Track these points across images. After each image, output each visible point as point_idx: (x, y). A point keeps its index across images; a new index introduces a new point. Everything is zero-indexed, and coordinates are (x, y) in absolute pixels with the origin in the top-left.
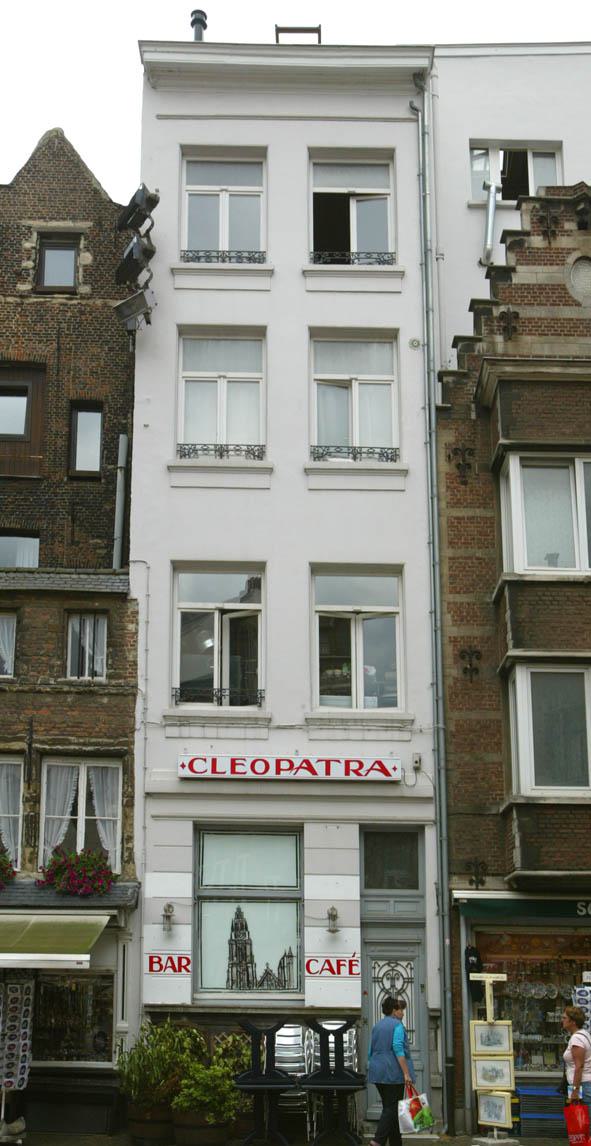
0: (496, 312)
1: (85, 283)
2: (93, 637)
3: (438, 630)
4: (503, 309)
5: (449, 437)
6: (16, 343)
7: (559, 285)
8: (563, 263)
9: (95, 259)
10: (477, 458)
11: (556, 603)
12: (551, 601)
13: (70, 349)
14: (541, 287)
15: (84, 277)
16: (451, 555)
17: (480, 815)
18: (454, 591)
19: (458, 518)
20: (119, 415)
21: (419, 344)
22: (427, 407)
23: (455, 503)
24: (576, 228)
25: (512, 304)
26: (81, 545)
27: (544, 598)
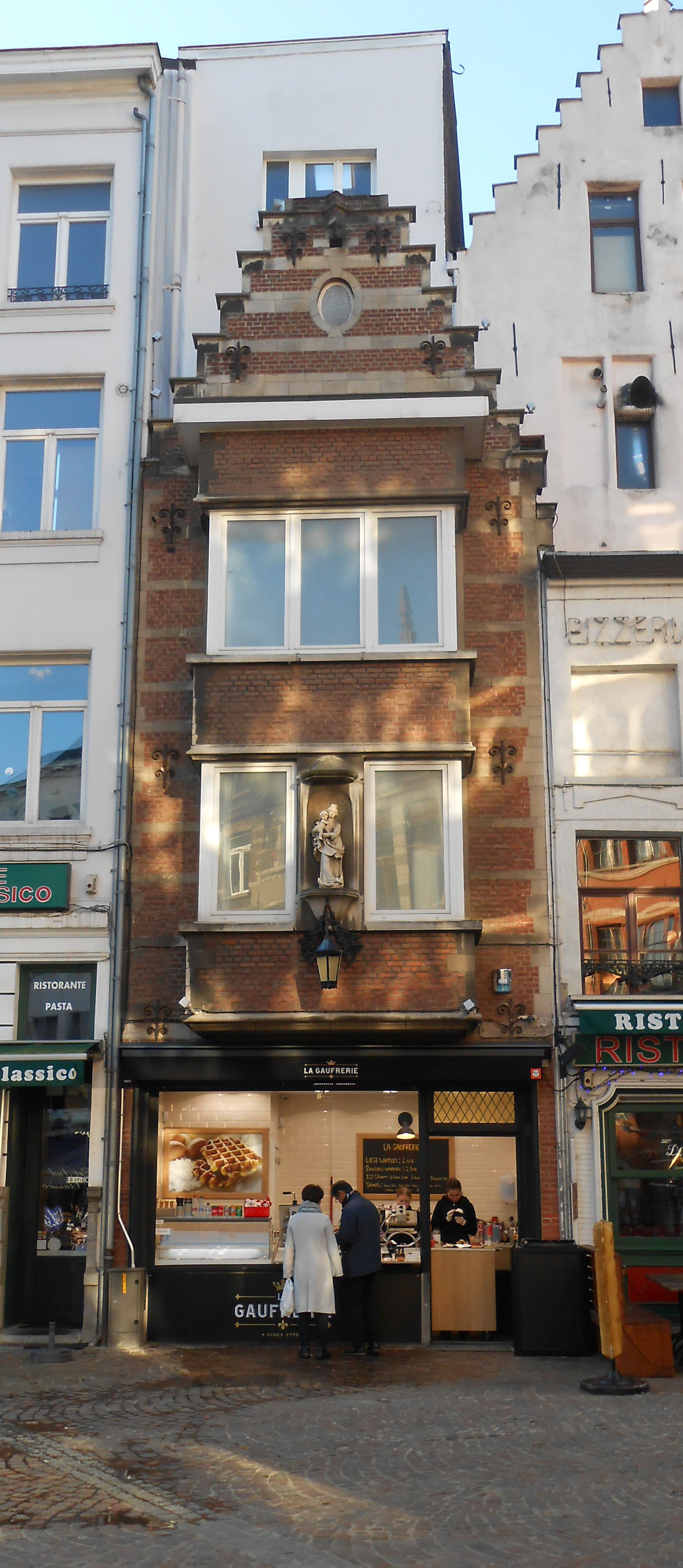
0: (222, 347)
4: (232, 343)
5: (154, 497)
7: (301, 313)
10: (188, 521)
11: (253, 688)
12: (247, 686)
14: (280, 317)
16: (149, 636)
17: (167, 948)
18: (150, 679)
19: (161, 593)
21: (127, 389)
22: (130, 463)
23: (159, 574)
24: (328, 245)
25: (244, 338)
27: (238, 683)
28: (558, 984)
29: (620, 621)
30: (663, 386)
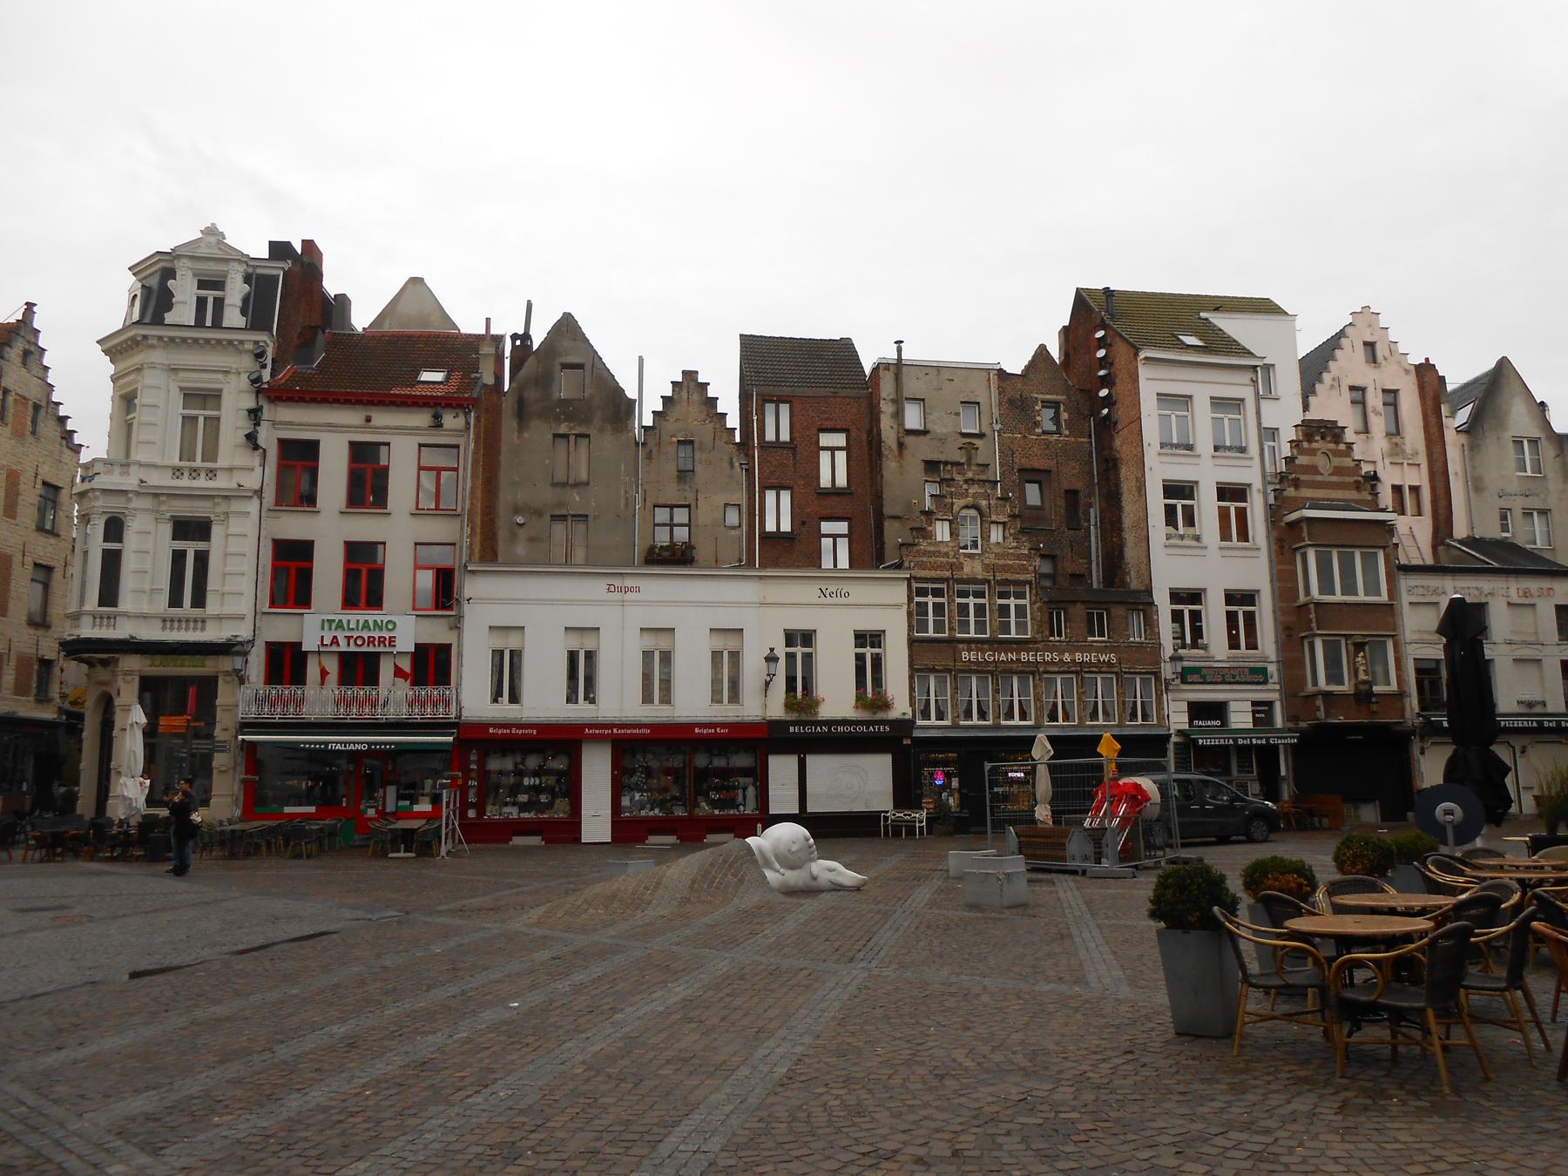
2: (1137, 621)
3: (1275, 619)
4: (1293, 476)
8: (1315, 455)
23: (1280, 563)
28: (1412, 709)
29: (1423, 587)
30: (1380, 474)
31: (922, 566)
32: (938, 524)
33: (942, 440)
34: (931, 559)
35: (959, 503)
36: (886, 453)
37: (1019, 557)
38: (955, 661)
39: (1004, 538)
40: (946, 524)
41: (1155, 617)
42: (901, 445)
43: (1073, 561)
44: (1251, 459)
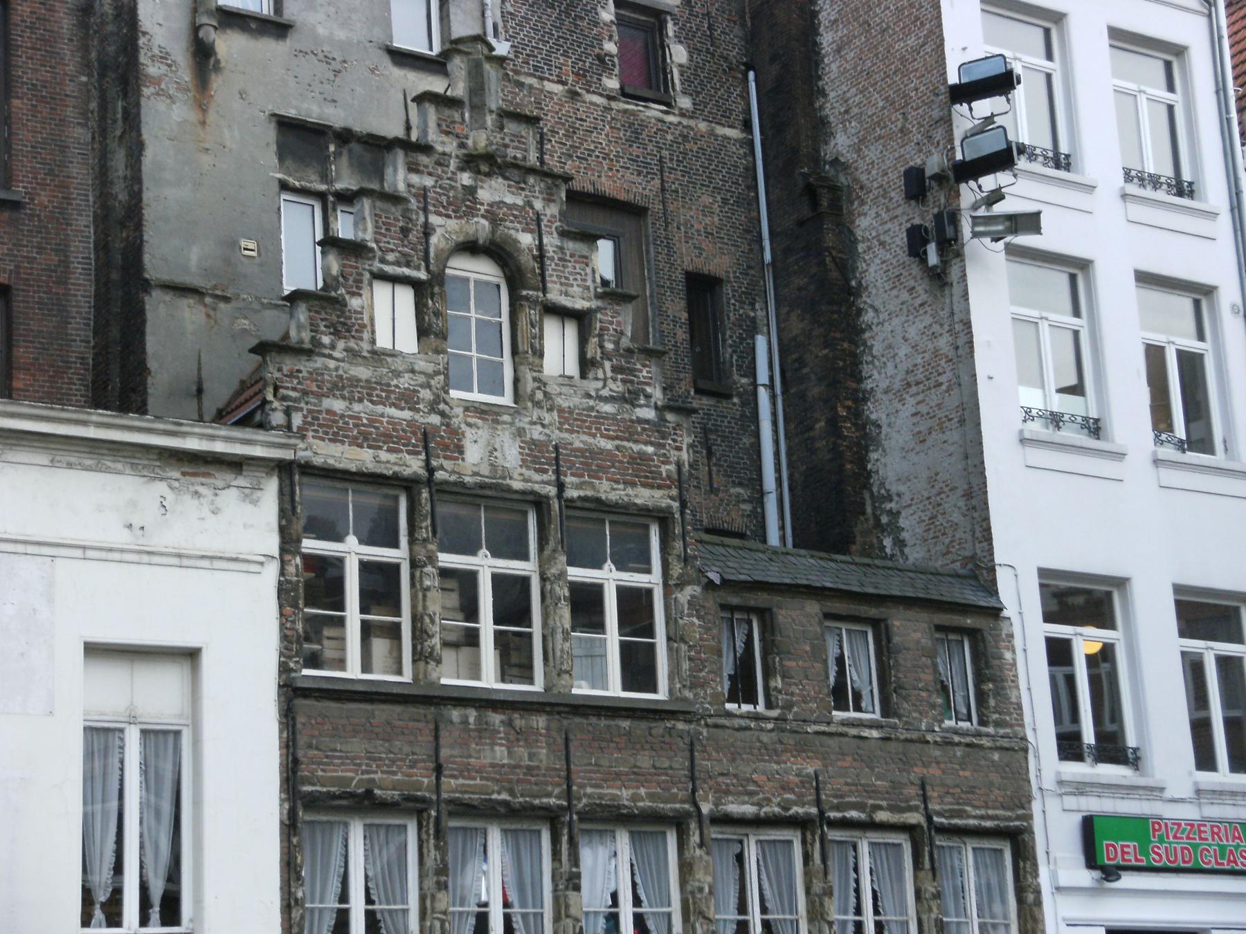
1: (684, 93)
6: (611, 169)
9: (690, 54)
13: (676, 191)
15: (682, 84)
20: (745, 303)
26: (721, 495)
31: (335, 430)
32: (382, 292)
33: (335, 65)
34: (357, 407)
35: (445, 229)
36: (153, 70)
37: (630, 431)
38: (439, 769)
39: (586, 364)
40: (406, 297)
41: (1008, 655)
42: (202, 54)
43: (713, 490)
44: (1213, 215)
